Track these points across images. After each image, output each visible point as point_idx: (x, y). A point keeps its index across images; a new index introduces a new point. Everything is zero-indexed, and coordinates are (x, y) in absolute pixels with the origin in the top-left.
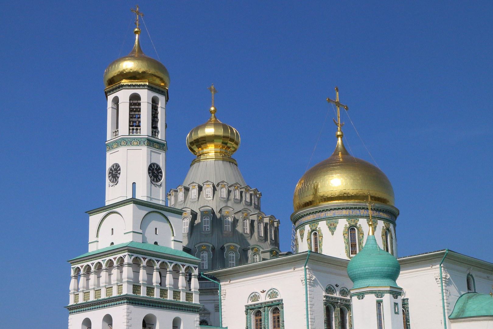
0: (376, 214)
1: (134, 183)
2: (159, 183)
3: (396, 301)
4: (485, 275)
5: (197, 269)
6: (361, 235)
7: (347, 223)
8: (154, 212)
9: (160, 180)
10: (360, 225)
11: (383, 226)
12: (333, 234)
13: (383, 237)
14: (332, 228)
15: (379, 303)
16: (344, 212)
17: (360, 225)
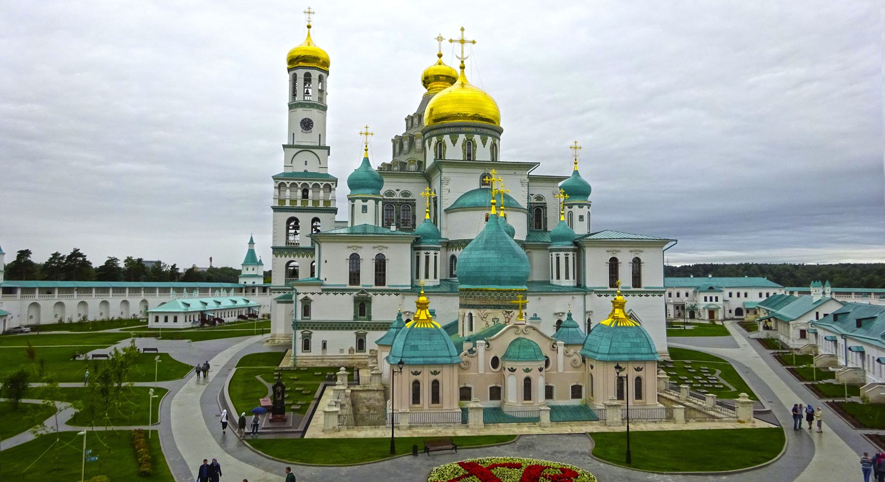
1: (294, 134)
2: (309, 131)
3: (365, 204)
4: (512, 172)
5: (335, 185)
6: (444, 148)
7: (436, 140)
9: (311, 129)
11: (464, 139)
14: (430, 145)
15: (353, 206)
16: (436, 132)
17: (444, 140)
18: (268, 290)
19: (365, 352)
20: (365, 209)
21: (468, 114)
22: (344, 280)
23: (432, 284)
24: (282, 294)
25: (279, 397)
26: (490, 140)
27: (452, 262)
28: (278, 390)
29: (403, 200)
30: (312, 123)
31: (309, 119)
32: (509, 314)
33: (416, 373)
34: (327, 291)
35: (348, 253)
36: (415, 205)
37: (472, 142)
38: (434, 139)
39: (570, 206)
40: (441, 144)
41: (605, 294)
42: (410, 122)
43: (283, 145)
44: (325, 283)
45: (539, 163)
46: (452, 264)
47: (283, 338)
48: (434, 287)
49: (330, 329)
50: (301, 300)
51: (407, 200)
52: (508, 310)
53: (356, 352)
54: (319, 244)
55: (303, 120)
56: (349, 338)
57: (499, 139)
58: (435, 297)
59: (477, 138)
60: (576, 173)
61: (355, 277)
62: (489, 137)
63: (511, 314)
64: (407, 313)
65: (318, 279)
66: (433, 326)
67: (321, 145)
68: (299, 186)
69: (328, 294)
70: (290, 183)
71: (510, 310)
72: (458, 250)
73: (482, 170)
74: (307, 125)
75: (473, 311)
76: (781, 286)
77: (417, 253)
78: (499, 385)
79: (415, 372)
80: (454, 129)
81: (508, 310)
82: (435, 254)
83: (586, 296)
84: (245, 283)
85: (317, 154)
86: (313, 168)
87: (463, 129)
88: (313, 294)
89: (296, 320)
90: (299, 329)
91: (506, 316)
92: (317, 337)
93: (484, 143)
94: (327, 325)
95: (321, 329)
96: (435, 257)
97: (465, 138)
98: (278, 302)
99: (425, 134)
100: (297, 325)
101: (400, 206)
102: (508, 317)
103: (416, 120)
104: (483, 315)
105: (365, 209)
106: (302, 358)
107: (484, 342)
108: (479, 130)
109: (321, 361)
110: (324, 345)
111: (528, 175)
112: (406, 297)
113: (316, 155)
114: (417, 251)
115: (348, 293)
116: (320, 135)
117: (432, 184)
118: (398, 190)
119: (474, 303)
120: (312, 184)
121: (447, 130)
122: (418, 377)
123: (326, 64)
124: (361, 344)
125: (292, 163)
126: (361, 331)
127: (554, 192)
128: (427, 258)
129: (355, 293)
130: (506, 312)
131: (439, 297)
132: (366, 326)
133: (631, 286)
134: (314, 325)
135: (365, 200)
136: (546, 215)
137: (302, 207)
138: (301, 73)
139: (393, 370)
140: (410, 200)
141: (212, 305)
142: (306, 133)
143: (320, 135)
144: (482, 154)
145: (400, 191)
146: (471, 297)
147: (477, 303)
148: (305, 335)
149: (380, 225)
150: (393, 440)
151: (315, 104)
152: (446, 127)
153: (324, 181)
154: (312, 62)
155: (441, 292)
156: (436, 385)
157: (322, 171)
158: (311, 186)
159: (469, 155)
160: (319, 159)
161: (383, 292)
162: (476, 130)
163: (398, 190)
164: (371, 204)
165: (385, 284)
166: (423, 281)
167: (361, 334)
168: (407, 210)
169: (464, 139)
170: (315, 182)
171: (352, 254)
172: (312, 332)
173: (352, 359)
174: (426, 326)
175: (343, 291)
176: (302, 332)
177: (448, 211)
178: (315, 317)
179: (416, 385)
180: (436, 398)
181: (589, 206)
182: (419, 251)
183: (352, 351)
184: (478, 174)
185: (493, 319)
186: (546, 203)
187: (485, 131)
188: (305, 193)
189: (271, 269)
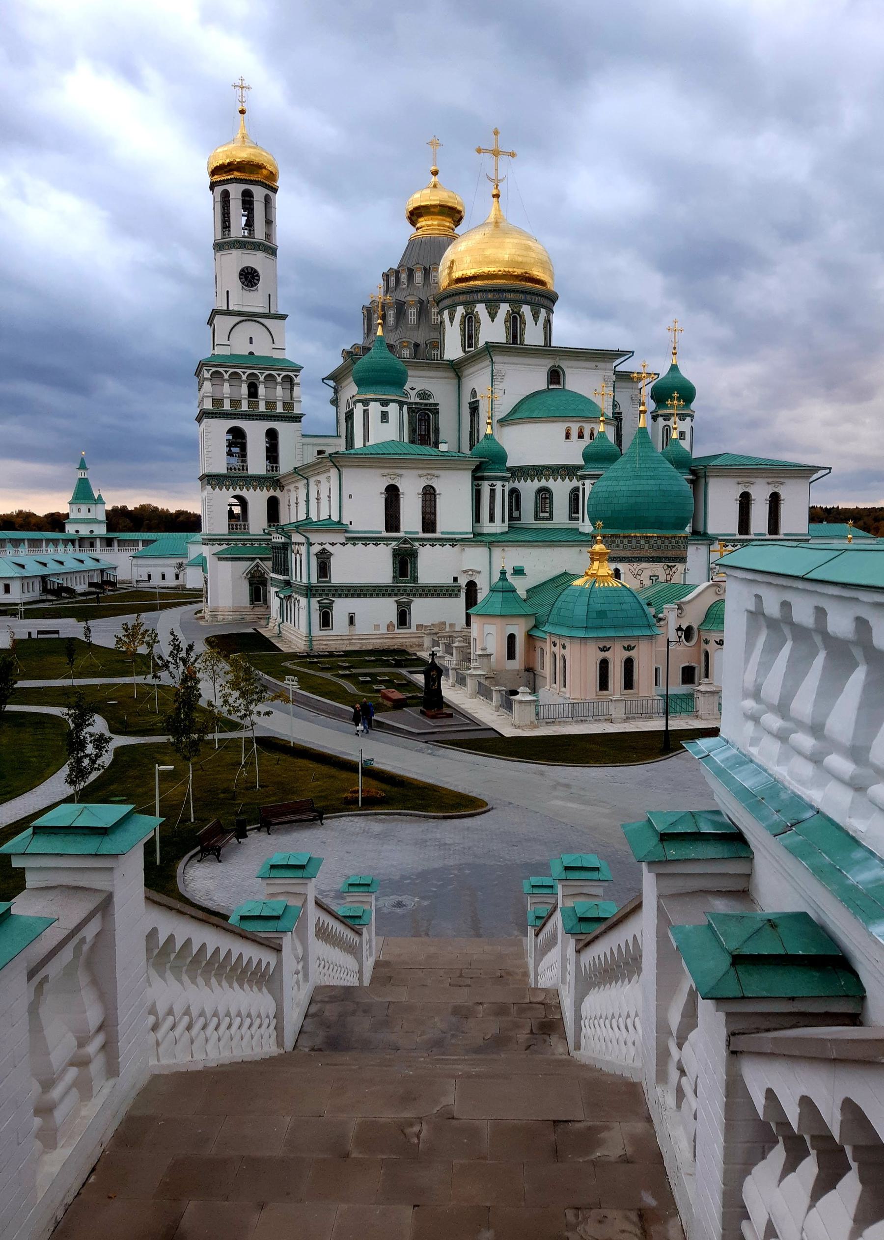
0: (496, 296)
1: (228, 292)
2: (255, 287)
3: (385, 409)
4: (593, 364)
8: (246, 320)
9: (256, 284)
10: (477, 312)
11: (508, 311)
12: (452, 325)
13: (508, 323)
14: (452, 320)
15: (366, 412)
16: (462, 298)
17: (477, 312)
18: (116, 544)
19: (410, 628)
20: (384, 417)
21: (515, 272)
22: (377, 523)
23: (499, 531)
24: (225, 546)
25: (434, 685)
26: (543, 312)
27: (512, 499)
28: (433, 675)
29: (421, 404)
30: (258, 275)
31: (252, 269)
32: (671, 569)
33: (604, 649)
34: (354, 540)
35: (381, 485)
36: (438, 413)
37: (520, 316)
38: (460, 310)
39: (667, 418)
40: (471, 317)
41: (733, 544)
42: (392, 279)
43: (288, 315)
44: (351, 528)
45: (633, 352)
46: (512, 502)
47: (231, 613)
48: (502, 534)
49: (353, 596)
50: (316, 554)
51: (426, 404)
52: (670, 564)
53: (398, 628)
54: (339, 471)
55: (243, 270)
56: (387, 608)
57: (553, 313)
58: (515, 549)
59: (526, 310)
60: (674, 368)
61: (392, 521)
62: (542, 309)
63: (674, 569)
64: (470, 573)
65: (339, 522)
66: (620, 585)
67: (272, 312)
68: (244, 377)
69: (354, 544)
70: (281, 376)
71: (673, 564)
72: (522, 481)
73: (548, 361)
74: (249, 277)
75: (620, 566)
76: (873, 536)
77: (476, 486)
78: (693, 664)
79: (604, 648)
80: (492, 294)
81: (670, 564)
82: (503, 486)
83: (711, 546)
84: (77, 531)
85: (268, 326)
86: (262, 349)
87: (507, 295)
88: (333, 544)
89: (310, 583)
90: (314, 596)
91: (667, 572)
92: (341, 607)
93: (536, 318)
94: (355, 591)
95: (347, 596)
96: (503, 490)
97: (510, 309)
98: (220, 559)
99: (440, 301)
100: (311, 591)
101: (417, 413)
102: (669, 574)
103: (404, 277)
104: (637, 570)
105: (384, 417)
106: (321, 638)
107: (673, 606)
108: (529, 297)
109: (348, 642)
110: (352, 620)
111: (615, 371)
112: (466, 549)
113: (263, 325)
114: (476, 483)
115: (384, 544)
116: (269, 295)
117: (464, 380)
118: (412, 389)
119: (622, 554)
120: (264, 375)
121: (480, 296)
122: (632, 654)
123: (273, 176)
124: (403, 618)
125: (229, 340)
126: (404, 599)
127: (633, 396)
128: (493, 491)
129: (394, 543)
130: (668, 566)
131: (519, 549)
132: (411, 591)
133: (767, 533)
134: (336, 591)
135: (385, 403)
136: (621, 431)
137: (249, 411)
138: (235, 191)
139: (668, 639)
140: (431, 404)
141: (53, 568)
142: (250, 290)
143: (269, 295)
144: (533, 335)
145: (415, 392)
146: (618, 546)
147: (628, 554)
148: (323, 605)
149: (406, 440)
150: (667, 733)
151: (261, 244)
152: (481, 291)
153: (282, 370)
154: (252, 173)
155: (522, 541)
156: (629, 664)
157: (276, 355)
158: (262, 378)
159: (515, 337)
160: (271, 335)
161: (433, 542)
162: (525, 297)
163: (412, 389)
164: (393, 409)
165: (435, 529)
166: (487, 528)
167: (404, 602)
168: (425, 420)
169: (508, 311)
170: (268, 372)
171: (425, 487)
172: (334, 601)
173: (393, 638)
174: (606, 585)
175: (376, 541)
176: (318, 601)
177: (503, 422)
178: (339, 576)
179: (604, 665)
180: (629, 683)
181: (692, 416)
182: (480, 482)
183: (391, 628)
184: (546, 366)
185: (650, 576)
186: (620, 413)
187: (537, 299)
188: (252, 390)
189: (68, 511)
